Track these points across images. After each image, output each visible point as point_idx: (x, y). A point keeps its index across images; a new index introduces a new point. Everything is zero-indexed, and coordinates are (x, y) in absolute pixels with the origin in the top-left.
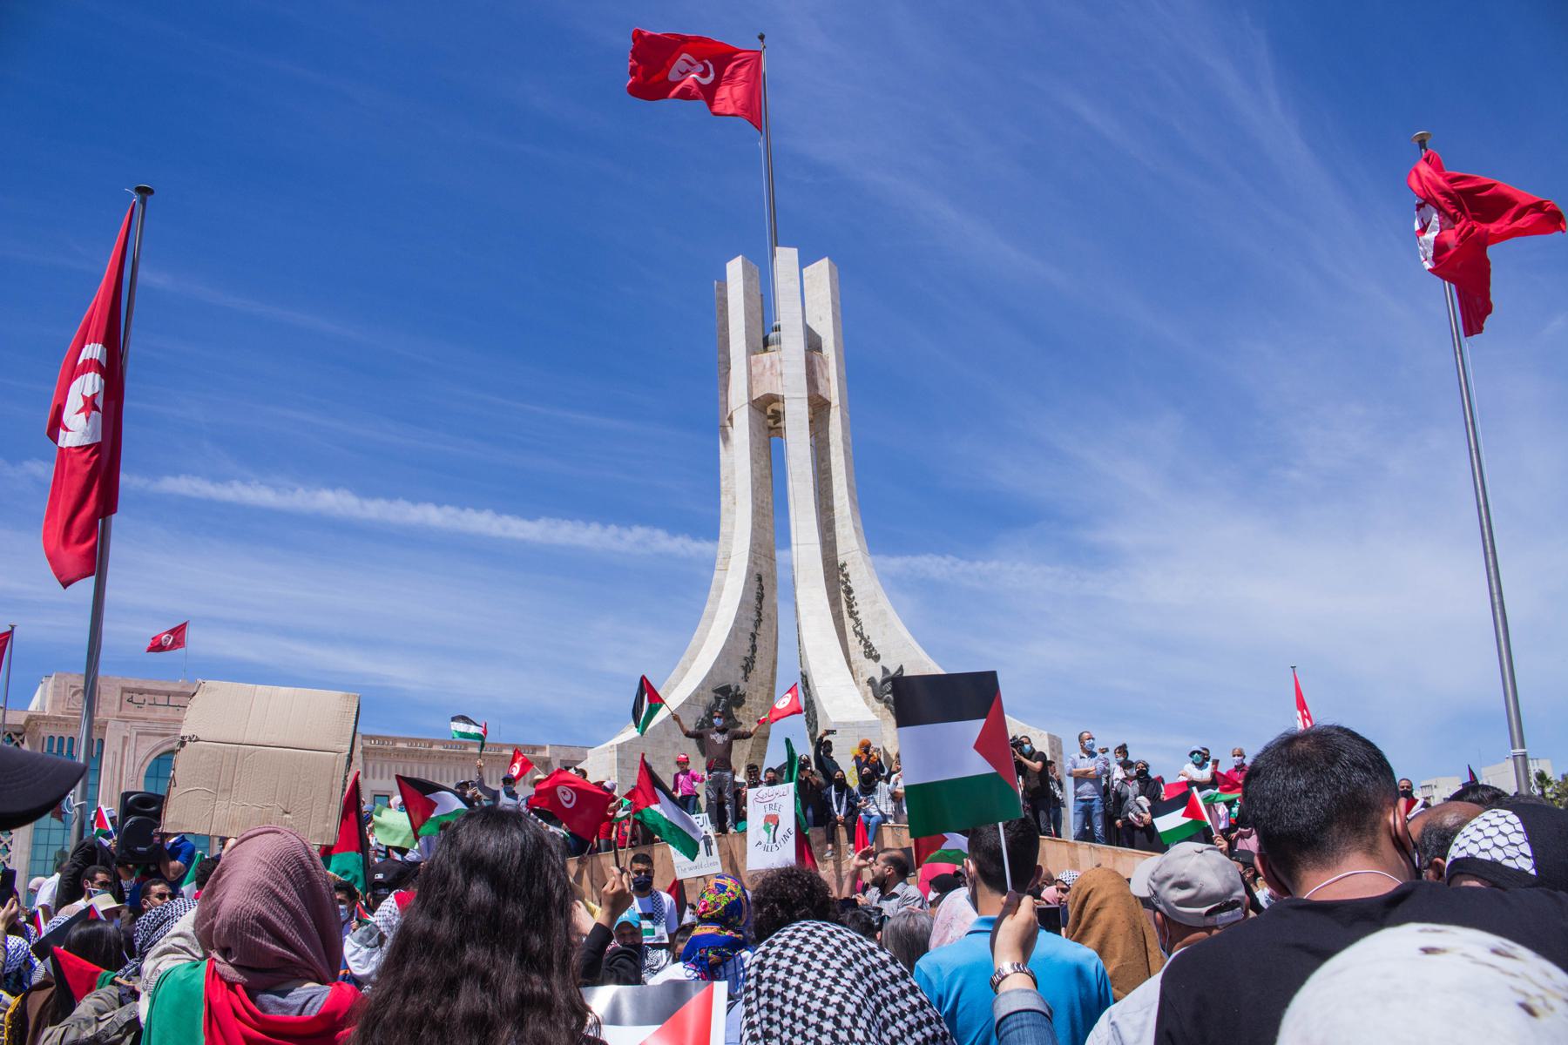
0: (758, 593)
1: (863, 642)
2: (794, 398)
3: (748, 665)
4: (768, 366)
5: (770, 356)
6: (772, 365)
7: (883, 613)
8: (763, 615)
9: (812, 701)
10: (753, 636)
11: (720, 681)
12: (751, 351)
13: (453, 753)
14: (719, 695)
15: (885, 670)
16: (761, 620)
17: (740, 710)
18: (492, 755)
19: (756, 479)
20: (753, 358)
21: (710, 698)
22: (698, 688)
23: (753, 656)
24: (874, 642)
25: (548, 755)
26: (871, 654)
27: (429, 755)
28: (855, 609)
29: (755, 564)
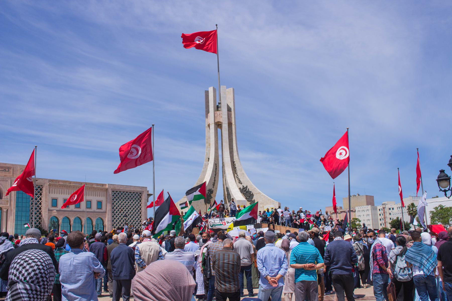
4: (219, 114)
6: (220, 115)
7: (243, 174)
9: (230, 194)
10: (215, 178)
12: (215, 111)
13: (78, 186)
15: (243, 186)
18: (89, 187)
20: (215, 112)
23: (215, 182)
24: (241, 180)
25: (107, 187)
26: (240, 182)
27: (70, 186)
28: (237, 172)
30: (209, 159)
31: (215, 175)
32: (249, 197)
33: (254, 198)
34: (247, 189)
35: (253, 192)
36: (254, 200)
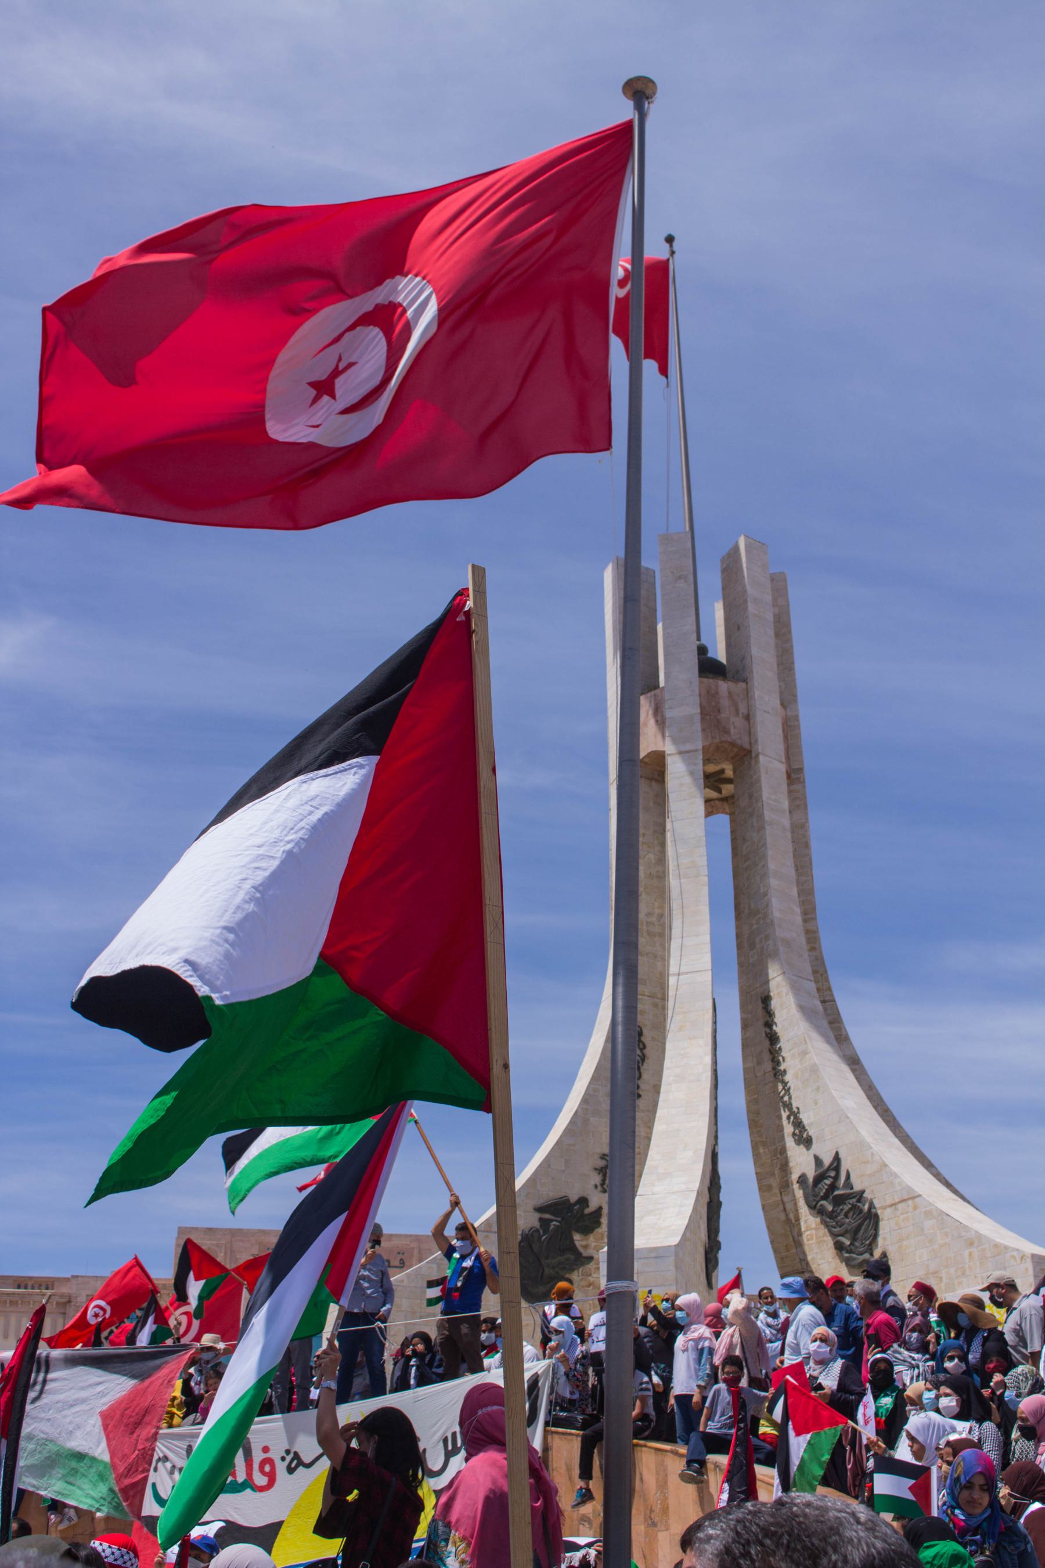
1: (792, 1118)
14: (547, 1216)
15: (818, 1161)
28: (782, 1068)
32: (854, 1239)
33: (880, 1240)
34: (837, 1178)
35: (879, 1197)
36: (884, 1255)
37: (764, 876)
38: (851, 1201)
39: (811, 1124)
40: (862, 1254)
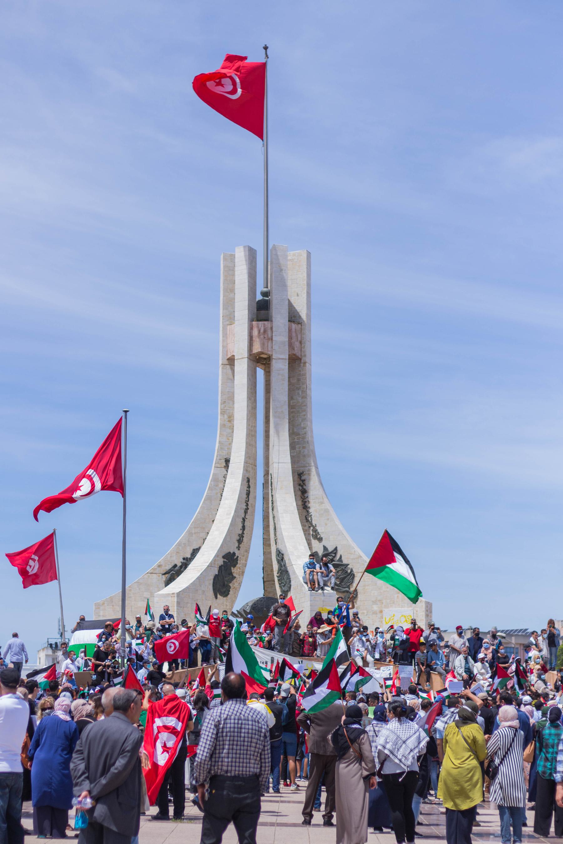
0: (247, 490)
2: (279, 359)
3: (240, 539)
5: (264, 324)
6: (265, 331)
7: (327, 511)
8: (249, 505)
9: (287, 572)
10: (244, 520)
11: (226, 551)
15: (325, 548)
16: (248, 509)
17: (235, 568)
19: (249, 411)
21: (221, 562)
22: (215, 556)
23: (243, 533)
24: (319, 529)
29: (247, 471)
30: (227, 461)
31: (246, 512)
34: (334, 557)
37: (304, 420)
38: (342, 567)
39: (323, 532)
40: (345, 588)
